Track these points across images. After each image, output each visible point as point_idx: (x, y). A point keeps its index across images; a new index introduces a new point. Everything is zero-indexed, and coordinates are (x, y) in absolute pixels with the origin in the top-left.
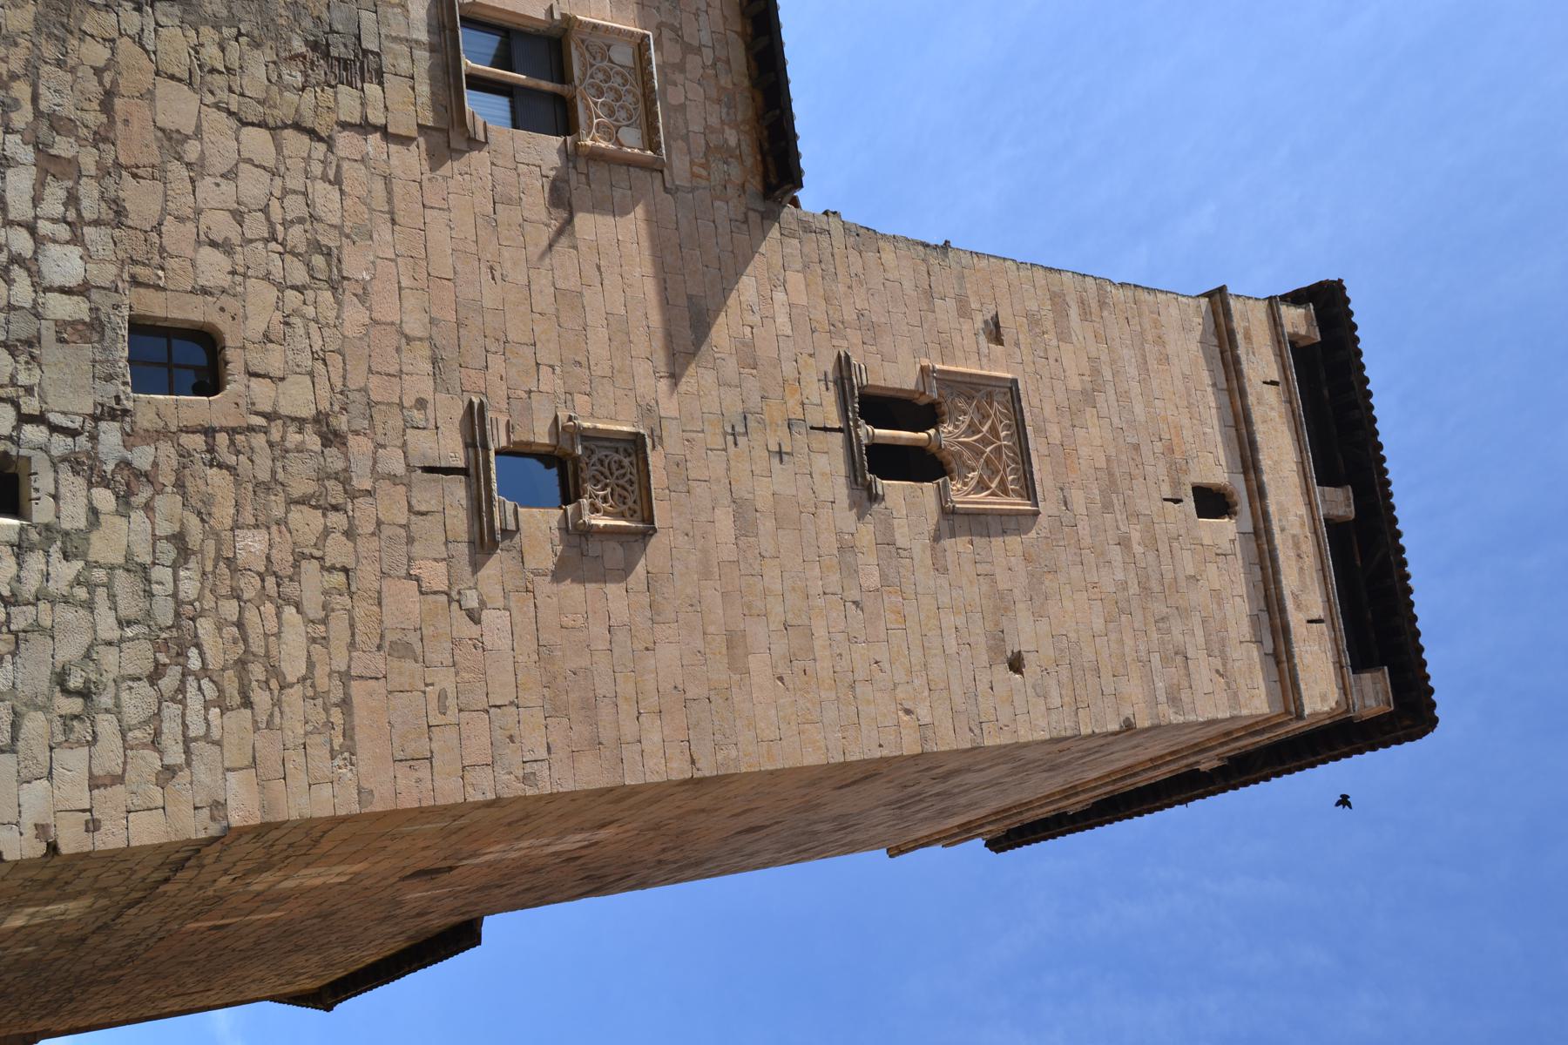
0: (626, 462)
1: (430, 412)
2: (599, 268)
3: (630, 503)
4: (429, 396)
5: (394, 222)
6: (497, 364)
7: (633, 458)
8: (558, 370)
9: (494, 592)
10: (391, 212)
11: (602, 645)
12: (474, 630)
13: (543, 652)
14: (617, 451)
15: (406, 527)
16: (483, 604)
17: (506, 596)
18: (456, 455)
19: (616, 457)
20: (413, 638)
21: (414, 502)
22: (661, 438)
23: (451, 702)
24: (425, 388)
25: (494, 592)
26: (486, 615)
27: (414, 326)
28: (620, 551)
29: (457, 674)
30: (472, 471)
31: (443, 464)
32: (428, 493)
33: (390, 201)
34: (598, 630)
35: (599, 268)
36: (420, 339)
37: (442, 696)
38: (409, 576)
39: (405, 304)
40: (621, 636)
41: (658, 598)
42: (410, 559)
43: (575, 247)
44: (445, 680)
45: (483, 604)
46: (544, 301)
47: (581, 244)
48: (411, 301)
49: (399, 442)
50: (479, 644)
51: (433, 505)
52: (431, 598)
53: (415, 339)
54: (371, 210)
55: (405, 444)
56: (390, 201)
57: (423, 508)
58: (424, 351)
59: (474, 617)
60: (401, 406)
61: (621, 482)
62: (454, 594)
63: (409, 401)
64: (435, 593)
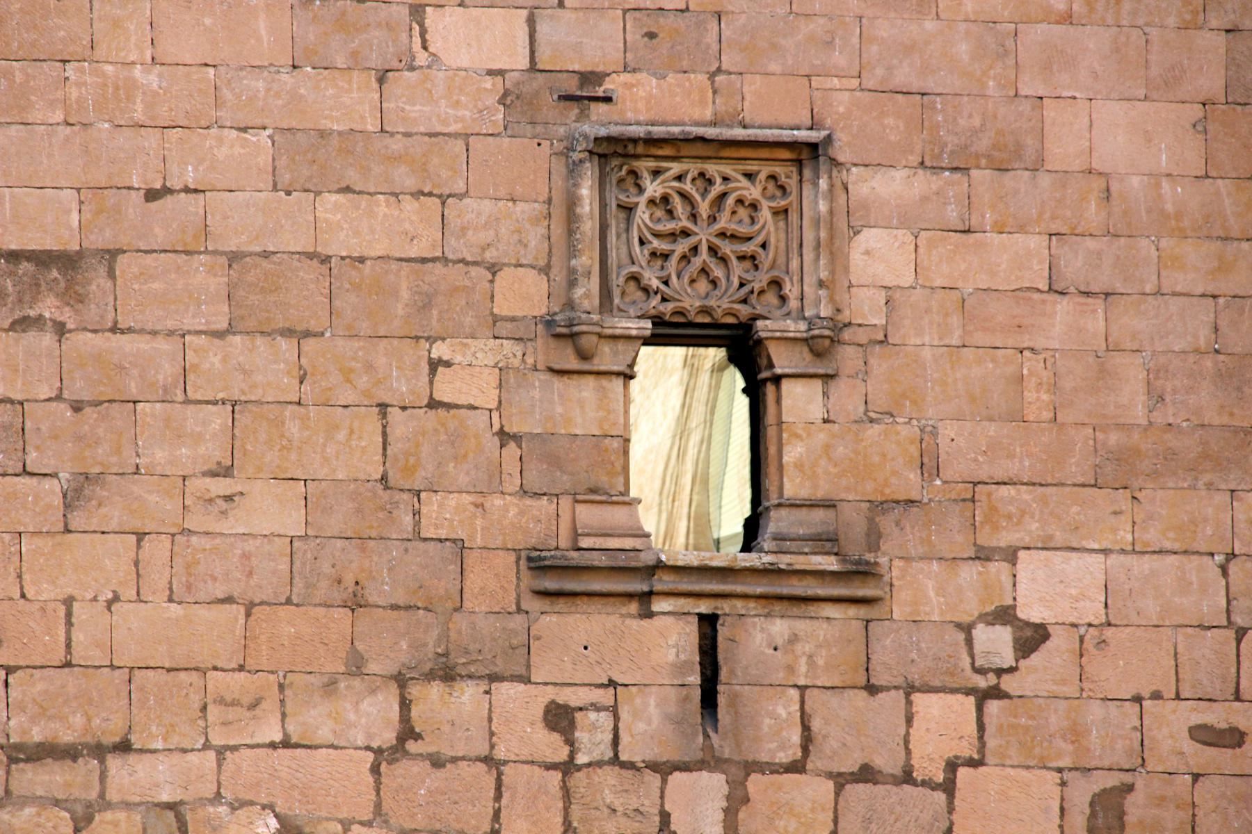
0: (653, 188)
1: (572, 697)
2: (152, 195)
3: (753, 192)
4: (541, 698)
5: (124, 747)
6: (444, 513)
7: (644, 166)
8: (440, 350)
9: (970, 587)
10: (99, 751)
11: (1095, 322)
12: (1059, 642)
13: (1118, 473)
14: (629, 209)
15: (841, 781)
16: (1004, 615)
17: (983, 555)
18: (669, 638)
19: (643, 215)
20: (1083, 792)
21: (783, 757)
22: (590, 78)
23: (1216, 716)
24: (520, 706)
25: (970, 587)
26: (1031, 612)
27: (374, 715)
28: (869, 238)
29: (1157, 696)
30: (704, 607)
31: (695, 679)
32: (772, 725)
33: (69, 753)
34: (1060, 322)
35: (152, 195)
36: (405, 705)
37: (1205, 735)
38: (949, 787)
39: (325, 734)
40: (1074, 265)
41: (983, 144)
42: (907, 777)
43: (112, 254)
44: (1172, 725)
45: (1004, 615)
46: (267, 366)
47: (100, 239)
48: (315, 719)
49: (654, 780)
50: (1091, 639)
51: (786, 708)
52: (991, 743)
53: (405, 718)
54: (104, 803)
55: (654, 767)
56: (69, 753)
57: (796, 738)
58: (431, 700)
59: (1032, 638)
60: (568, 767)
61: (704, 208)
62: (982, 682)
63: (552, 747)
64: (981, 727)
